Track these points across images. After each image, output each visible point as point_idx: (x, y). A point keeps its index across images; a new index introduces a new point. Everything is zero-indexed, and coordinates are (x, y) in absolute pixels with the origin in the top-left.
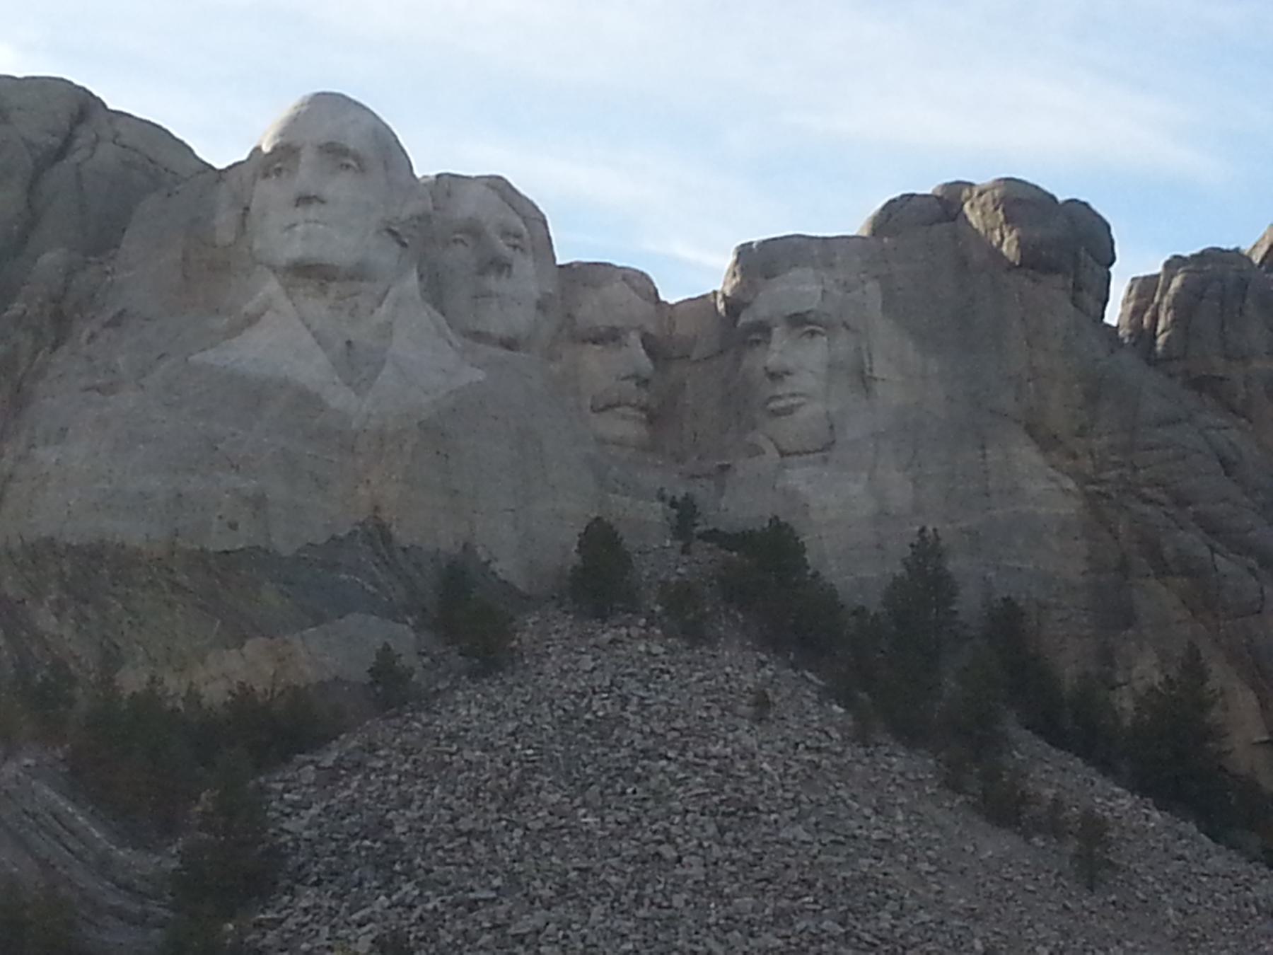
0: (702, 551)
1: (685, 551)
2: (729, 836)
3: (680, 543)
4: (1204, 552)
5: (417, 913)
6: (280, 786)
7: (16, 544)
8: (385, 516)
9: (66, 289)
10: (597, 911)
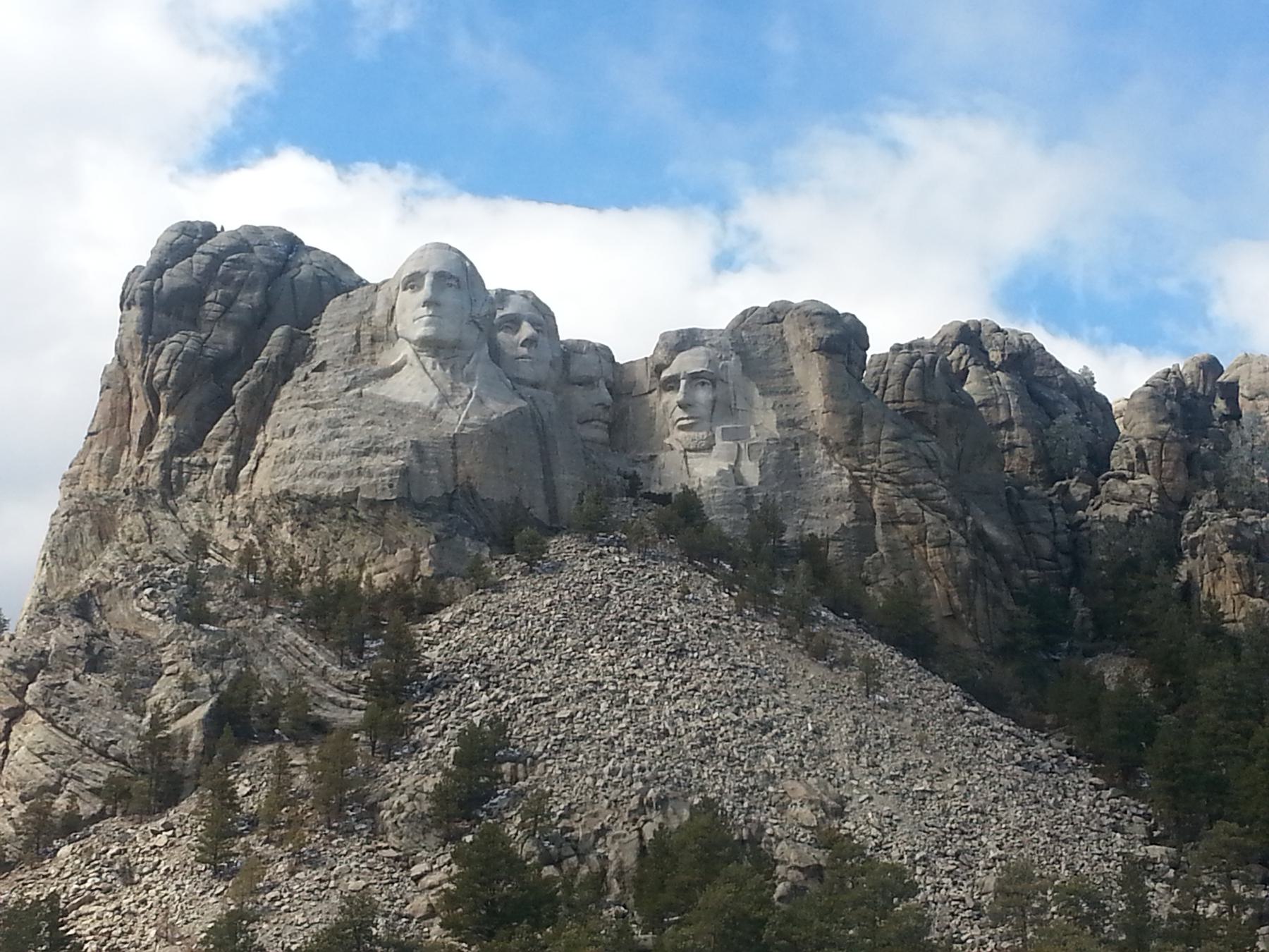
0: (644, 503)
1: (635, 504)
2: (672, 665)
3: (631, 500)
4: (919, 510)
5: (505, 704)
6: (421, 632)
7: (267, 493)
9: (290, 349)
10: (604, 706)
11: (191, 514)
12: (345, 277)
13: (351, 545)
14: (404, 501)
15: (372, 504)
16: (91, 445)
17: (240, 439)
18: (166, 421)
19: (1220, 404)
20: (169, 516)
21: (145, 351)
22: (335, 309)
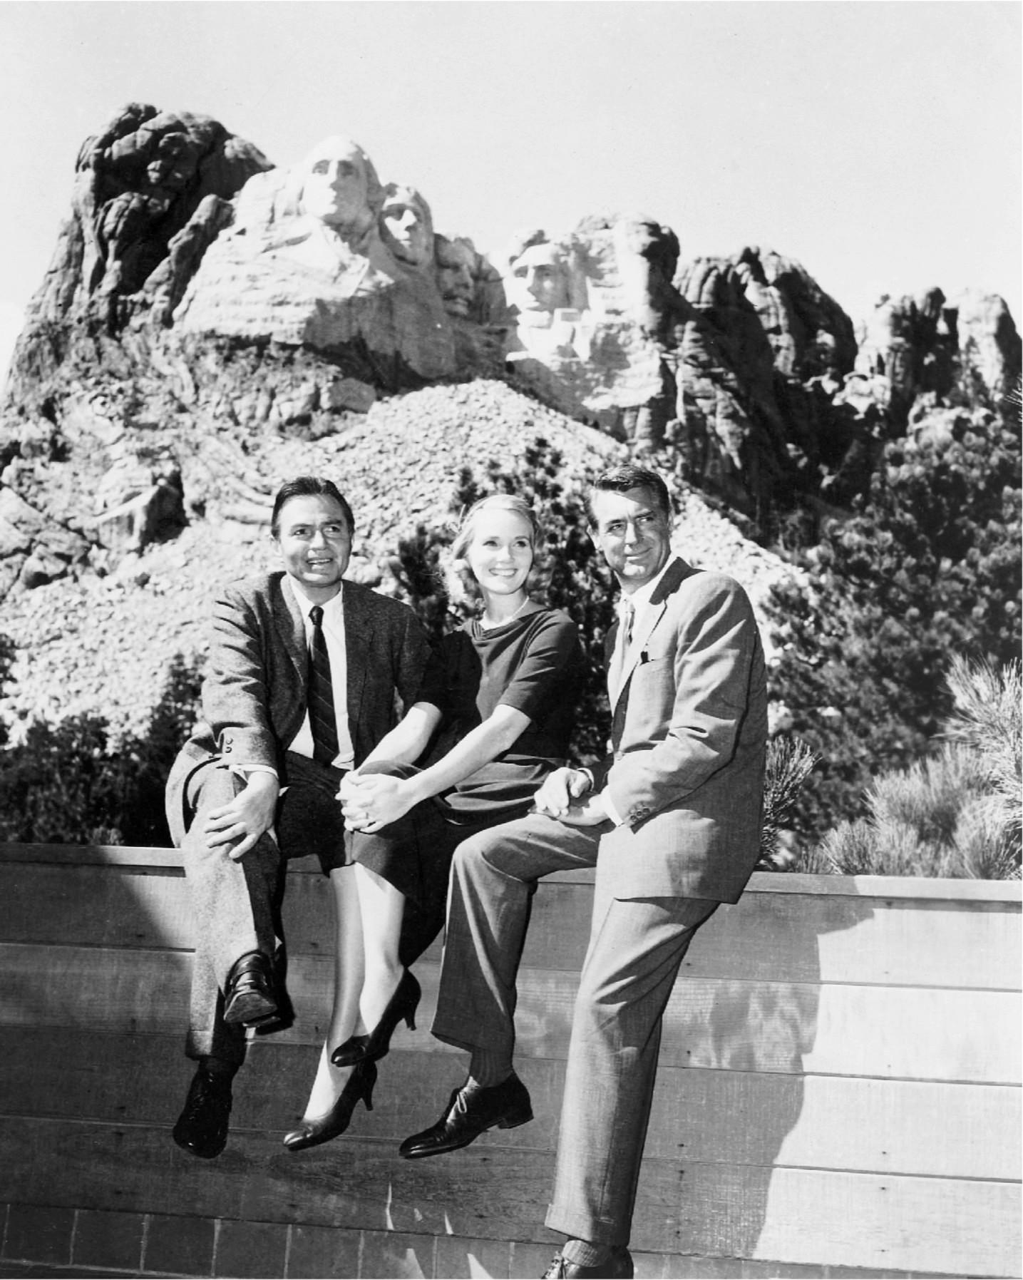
4: (711, 388)
7: (196, 331)
8: (364, 336)
11: (131, 340)
12: (260, 161)
13: (264, 378)
14: (308, 347)
15: (283, 346)
16: (50, 282)
17: (175, 285)
18: (113, 265)
19: (942, 327)
20: (115, 343)
21: (96, 206)
22: (254, 183)
